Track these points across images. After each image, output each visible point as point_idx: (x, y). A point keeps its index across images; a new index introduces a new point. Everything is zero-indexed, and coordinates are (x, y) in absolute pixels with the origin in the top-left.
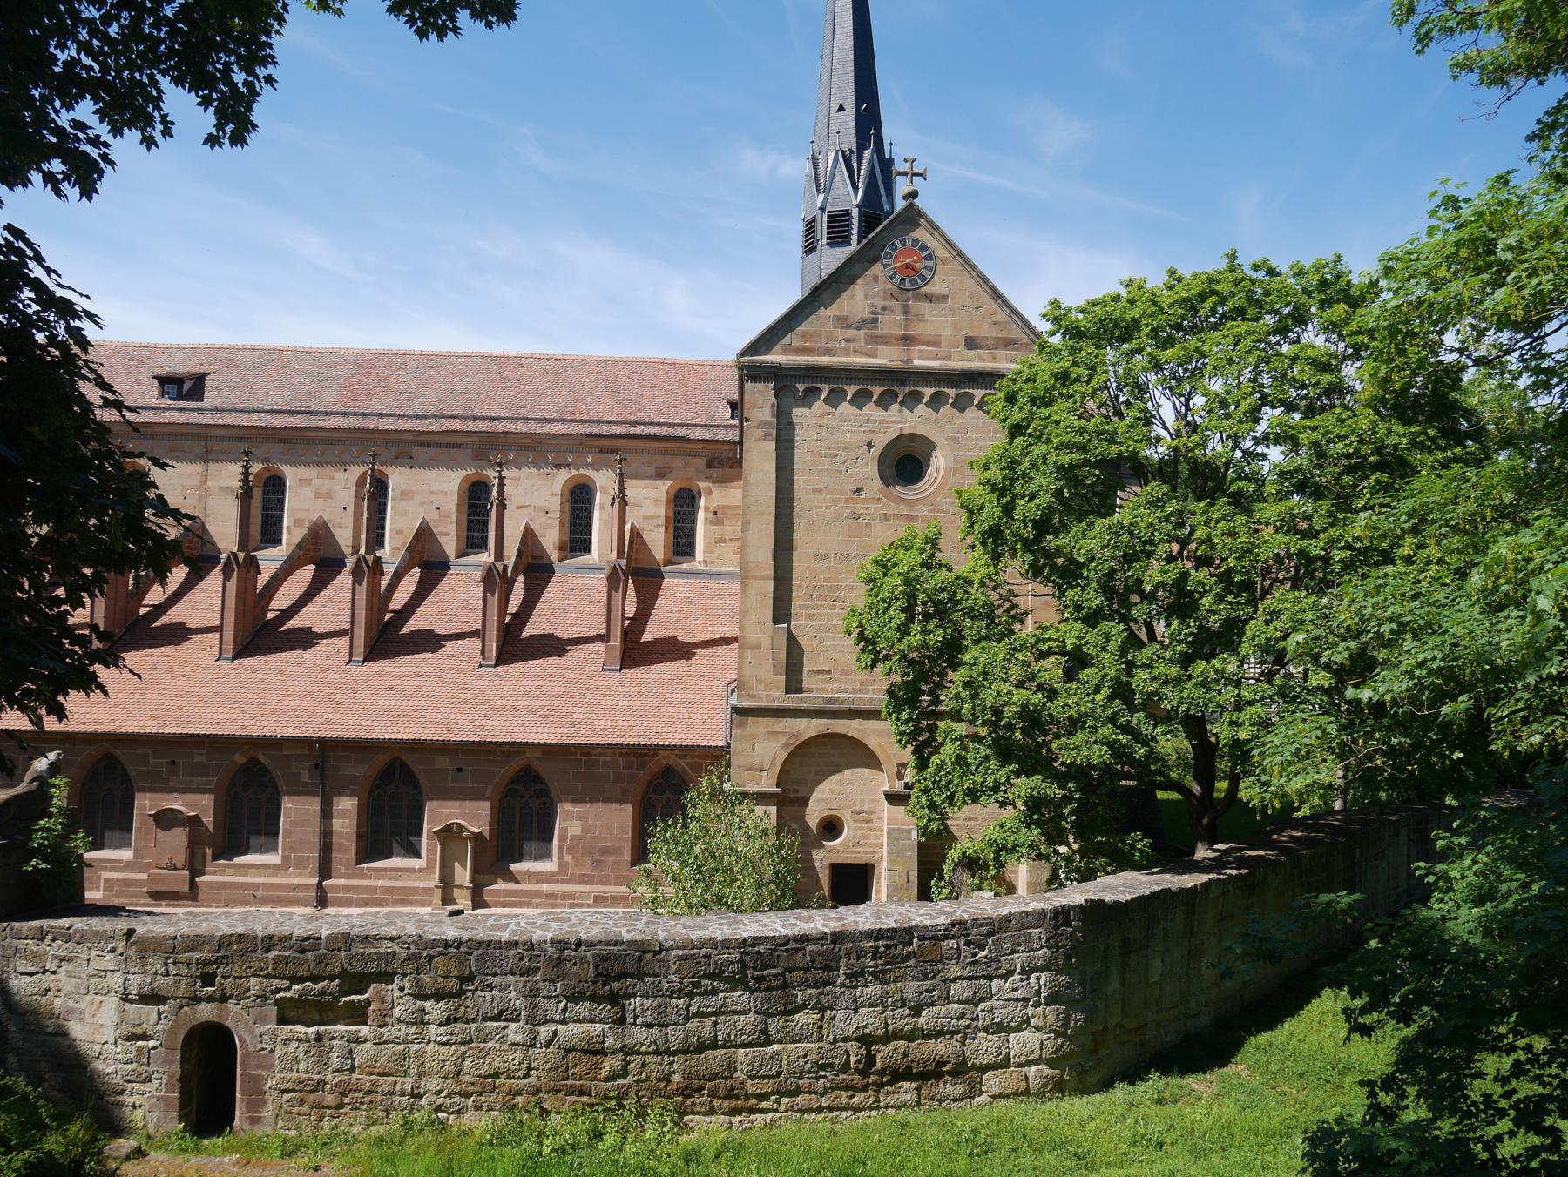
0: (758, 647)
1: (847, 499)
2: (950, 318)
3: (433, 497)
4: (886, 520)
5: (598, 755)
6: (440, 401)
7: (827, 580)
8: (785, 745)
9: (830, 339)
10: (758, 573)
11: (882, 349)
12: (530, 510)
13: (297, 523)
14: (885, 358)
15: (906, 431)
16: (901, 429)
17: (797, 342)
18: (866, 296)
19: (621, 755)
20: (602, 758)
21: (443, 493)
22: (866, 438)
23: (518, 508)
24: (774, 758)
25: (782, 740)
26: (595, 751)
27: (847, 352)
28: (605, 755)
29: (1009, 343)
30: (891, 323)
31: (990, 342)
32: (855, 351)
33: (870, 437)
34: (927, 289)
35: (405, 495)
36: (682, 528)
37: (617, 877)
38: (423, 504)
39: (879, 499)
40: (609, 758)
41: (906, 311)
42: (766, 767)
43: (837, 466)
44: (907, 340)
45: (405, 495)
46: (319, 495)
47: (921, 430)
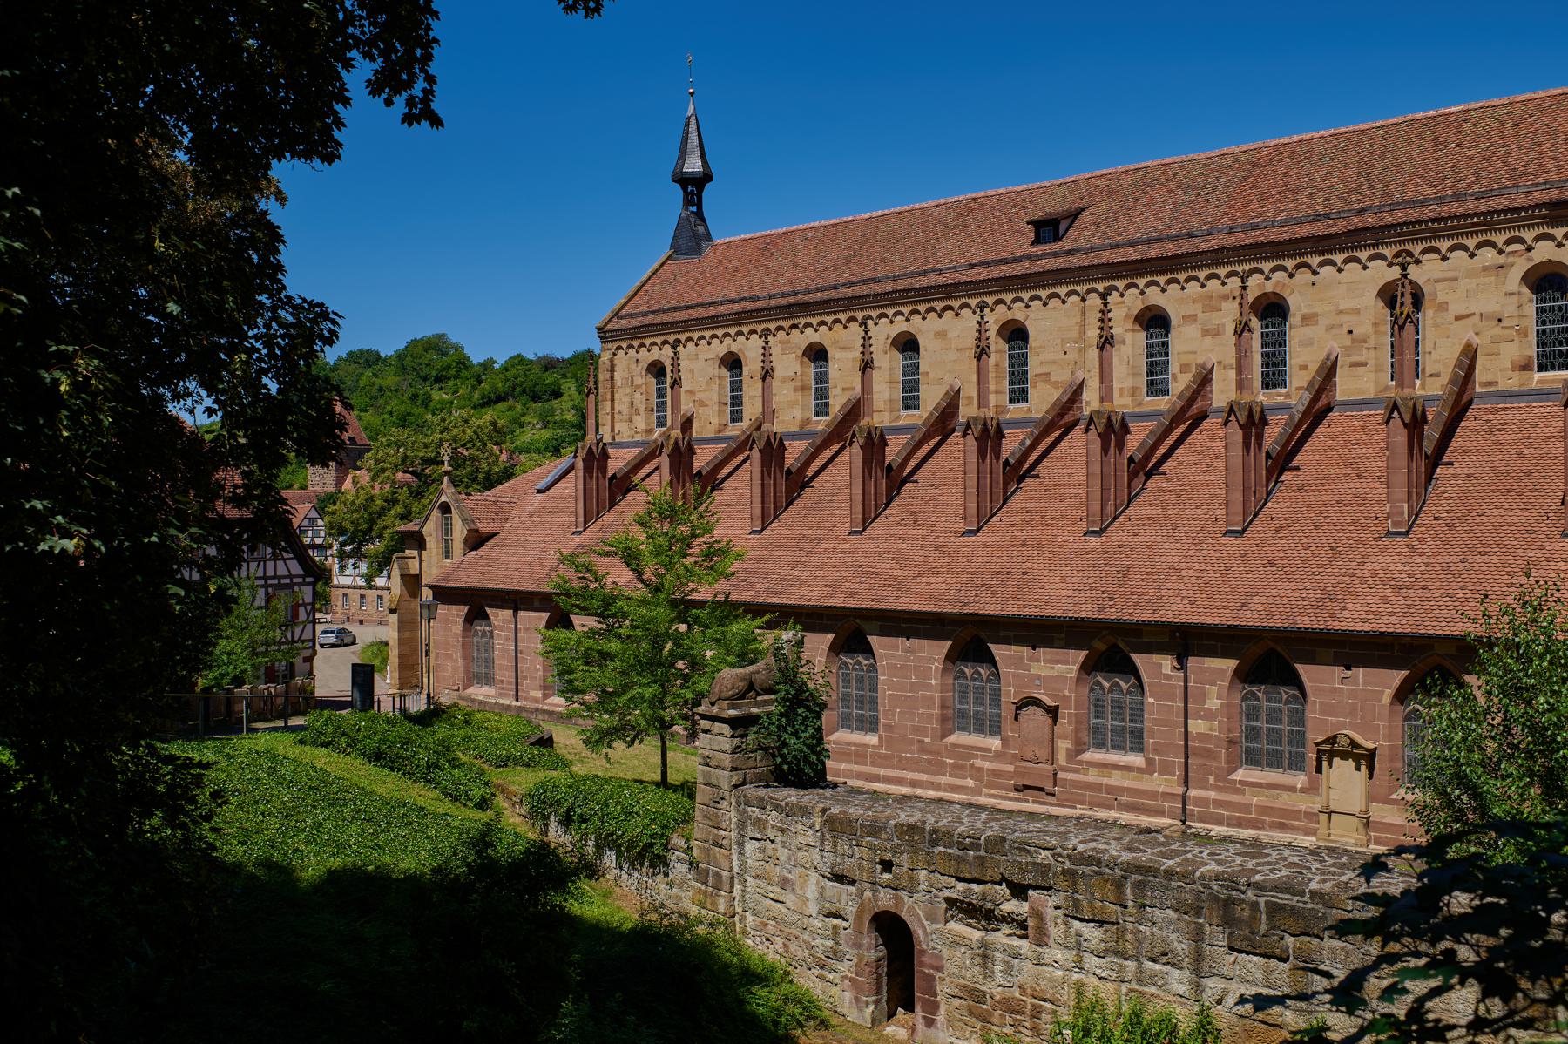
3: (1344, 318)
6: (1350, 192)
12: (1476, 319)
13: (1184, 368)
21: (1357, 311)
23: (1457, 318)
35: (1308, 319)
38: (1330, 328)
45: (1308, 319)
46: (1206, 333)
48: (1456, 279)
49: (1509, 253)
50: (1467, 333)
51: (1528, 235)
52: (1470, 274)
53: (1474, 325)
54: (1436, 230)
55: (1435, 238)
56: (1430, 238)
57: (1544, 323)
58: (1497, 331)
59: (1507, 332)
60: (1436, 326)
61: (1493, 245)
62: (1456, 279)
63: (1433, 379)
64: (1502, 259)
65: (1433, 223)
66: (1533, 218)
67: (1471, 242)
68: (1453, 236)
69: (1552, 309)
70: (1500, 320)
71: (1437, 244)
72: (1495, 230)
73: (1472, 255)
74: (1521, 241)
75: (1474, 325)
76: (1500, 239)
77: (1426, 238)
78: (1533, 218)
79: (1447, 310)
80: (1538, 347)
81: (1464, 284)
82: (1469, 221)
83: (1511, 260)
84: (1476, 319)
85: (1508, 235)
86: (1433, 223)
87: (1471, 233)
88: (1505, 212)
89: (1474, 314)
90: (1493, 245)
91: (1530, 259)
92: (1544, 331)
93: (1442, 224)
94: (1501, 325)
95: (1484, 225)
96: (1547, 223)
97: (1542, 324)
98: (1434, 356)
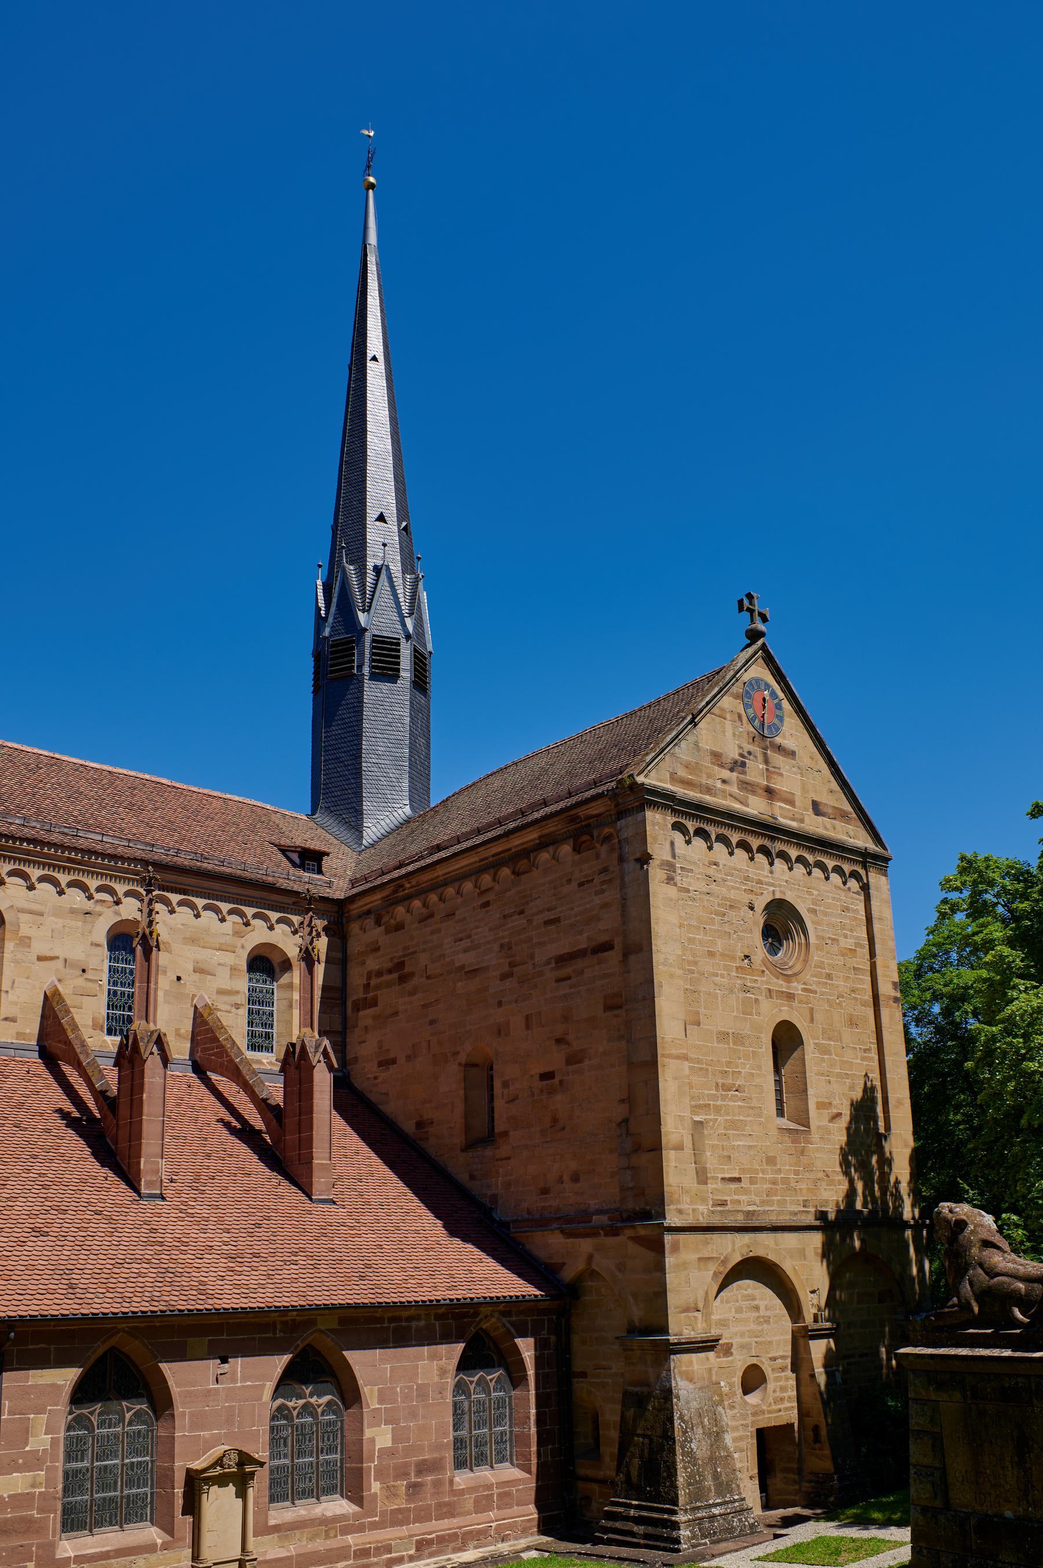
0: (679, 1147)
1: (737, 968)
2: (799, 777)
4: (771, 997)
5: (410, 1319)
7: (729, 1064)
8: (715, 1274)
9: (709, 776)
10: (674, 1052)
11: (753, 799)
12: (59, 964)
14: (755, 807)
15: (778, 896)
16: (774, 892)
17: (682, 773)
18: (734, 734)
19: (438, 1317)
20: (414, 1324)
22: (746, 898)
23: (40, 959)
24: (707, 1293)
25: (713, 1267)
26: (405, 1314)
27: (725, 794)
28: (418, 1318)
29: (843, 816)
30: (755, 772)
31: (830, 811)
32: (731, 795)
33: (752, 897)
34: (778, 740)
36: (258, 1012)
37: (440, 1506)
39: (763, 971)
40: (422, 1323)
41: (766, 761)
42: (701, 1306)
43: (727, 928)
44: (770, 793)
47: (790, 897)
48: (41, 914)
49: (98, 901)
50: (46, 978)
51: (121, 888)
52: (57, 912)
53: (57, 970)
54: (28, 852)
55: (25, 861)
56: (20, 860)
57: (115, 984)
58: (80, 982)
59: (90, 985)
60: (16, 962)
61: (84, 888)
62: (41, 914)
63: (8, 1023)
64: (89, 905)
65: (29, 844)
66: (127, 871)
67: (63, 878)
68: (44, 865)
69: (124, 970)
70: (84, 971)
71: (28, 870)
72: (89, 872)
73: (61, 893)
74: (112, 892)
75: (57, 970)
76: (93, 883)
77: (15, 859)
78: (127, 871)
79: (29, 947)
80: (108, 1009)
81: (51, 922)
82: (66, 854)
83: (99, 908)
84: (59, 964)
85: (72, 877)
86: (29, 844)
87: (64, 868)
88: (104, 855)
89: (58, 958)
90: (84, 888)
91: (117, 913)
92: (115, 992)
93: (38, 849)
94: (86, 976)
95: (79, 864)
96: (137, 880)
97: (114, 985)
98: (11, 997)
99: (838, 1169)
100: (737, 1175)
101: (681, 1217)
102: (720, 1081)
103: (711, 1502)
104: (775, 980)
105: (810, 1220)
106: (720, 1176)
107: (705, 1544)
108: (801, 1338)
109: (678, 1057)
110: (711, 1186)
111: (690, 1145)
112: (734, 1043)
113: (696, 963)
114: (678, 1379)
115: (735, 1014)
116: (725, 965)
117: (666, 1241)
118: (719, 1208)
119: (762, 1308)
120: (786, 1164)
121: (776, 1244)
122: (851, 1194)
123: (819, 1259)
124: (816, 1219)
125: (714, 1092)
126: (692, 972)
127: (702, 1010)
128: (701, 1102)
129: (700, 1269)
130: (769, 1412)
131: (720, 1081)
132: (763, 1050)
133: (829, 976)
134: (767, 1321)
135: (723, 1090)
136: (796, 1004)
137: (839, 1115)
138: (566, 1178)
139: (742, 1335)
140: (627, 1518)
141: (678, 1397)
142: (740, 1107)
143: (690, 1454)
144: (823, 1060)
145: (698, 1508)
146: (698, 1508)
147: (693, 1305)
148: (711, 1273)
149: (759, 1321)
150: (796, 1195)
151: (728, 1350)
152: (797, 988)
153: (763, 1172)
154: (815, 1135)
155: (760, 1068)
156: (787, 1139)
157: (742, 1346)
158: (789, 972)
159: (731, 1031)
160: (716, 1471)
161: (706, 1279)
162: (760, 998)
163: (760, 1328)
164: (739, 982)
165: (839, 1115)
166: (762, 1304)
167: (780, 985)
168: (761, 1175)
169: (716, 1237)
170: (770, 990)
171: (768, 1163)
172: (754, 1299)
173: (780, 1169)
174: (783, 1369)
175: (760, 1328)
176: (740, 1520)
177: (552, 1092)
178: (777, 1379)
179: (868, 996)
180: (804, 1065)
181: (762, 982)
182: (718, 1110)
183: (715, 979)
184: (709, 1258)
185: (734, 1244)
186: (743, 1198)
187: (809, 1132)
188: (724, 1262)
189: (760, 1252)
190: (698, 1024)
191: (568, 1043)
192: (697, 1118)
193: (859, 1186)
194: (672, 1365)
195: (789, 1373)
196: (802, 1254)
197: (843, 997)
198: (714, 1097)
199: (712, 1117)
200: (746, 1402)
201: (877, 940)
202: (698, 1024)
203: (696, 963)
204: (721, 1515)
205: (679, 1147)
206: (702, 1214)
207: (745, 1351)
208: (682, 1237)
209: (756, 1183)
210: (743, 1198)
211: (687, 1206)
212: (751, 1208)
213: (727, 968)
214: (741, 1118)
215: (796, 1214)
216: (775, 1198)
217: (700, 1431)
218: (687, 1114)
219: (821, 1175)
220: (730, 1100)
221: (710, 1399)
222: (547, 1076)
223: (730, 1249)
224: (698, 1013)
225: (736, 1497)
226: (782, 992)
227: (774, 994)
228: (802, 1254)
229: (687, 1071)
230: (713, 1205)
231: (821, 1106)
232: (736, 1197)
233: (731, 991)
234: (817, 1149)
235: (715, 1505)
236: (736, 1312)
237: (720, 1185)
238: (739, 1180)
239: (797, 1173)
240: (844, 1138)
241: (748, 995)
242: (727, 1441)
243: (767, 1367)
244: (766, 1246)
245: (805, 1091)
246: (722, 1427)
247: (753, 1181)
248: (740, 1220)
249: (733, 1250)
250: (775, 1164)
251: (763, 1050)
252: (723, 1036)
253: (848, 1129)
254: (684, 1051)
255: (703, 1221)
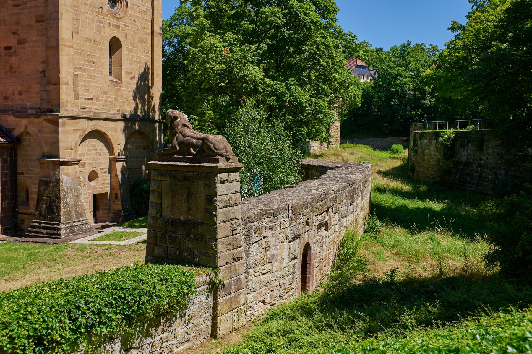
0: (67, 84)
1: (96, 12)
4: (110, 26)
7: (90, 52)
8: (80, 136)
10: (67, 44)
24: (76, 143)
25: (79, 133)
39: (107, 15)
42: (73, 148)
99: (132, 98)
100: (91, 98)
101: (67, 112)
102: (86, 59)
103: (74, 221)
104: (112, 19)
105: (119, 117)
106: (84, 97)
107: (71, 236)
108: (113, 161)
109: (68, 46)
110: (80, 101)
111: (72, 84)
112: (93, 43)
113: (78, 7)
114: (63, 175)
115: (94, 31)
116: (91, 10)
117: (60, 122)
118: (83, 110)
119: (98, 150)
120: (111, 95)
121: (105, 125)
122: (136, 108)
123: (122, 132)
124: (122, 117)
125: (83, 63)
126: (76, 10)
127: (80, 28)
128: (78, 66)
129: (74, 134)
130: (99, 188)
131: (86, 59)
132: (105, 48)
133: (135, 21)
134: (100, 154)
135: (87, 62)
136: (120, 30)
137: (134, 77)
138: (16, 93)
139: (90, 159)
140: (39, 227)
141: (62, 182)
142: (94, 70)
143: (67, 203)
144: (130, 55)
145: (69, 223)
146: (69, 223)
147: (70, 147)
148: (78, 135)
149: (96, 154)
150: (115, 107)
151: (84, 165)
152: (121, 23)
153: (102, 97)
154: (124, 84)
155: (103, 55)
156: (112, 85)
157: (90, 164)
158: (118, 17)
159: (92, 38)
160: (77, 209)
161: (76, 137)
162: (105, 26)
163: (97, 157)
164: (97, 18)
165: (134, 77)
166: (98, 148)
167: (114, 21)
168: (101, 98)
169: (81, 121)
170: (110, 23)
171: (104, 94)
172: (95, 146)
173: (109, 97)
174: (105, 173)
175: (97, 157)
176: (85, 227)
177: (10, 55)
178: (102, 176)
179: (150, 31)
180: (122, 56)
181: (107, 19)
182: (85, 70)
183: (86, 15)
184: (78, 129)
185: (88, 124)
186: (93, 107)
187: (122, 83)
188: (84, 131)
189: (99, 128)
190: (78, 33)
191: (18, 35)
192: (75, 73)
193: (140, 106)
194: (60, 170)
195: (107, 174)
196: (115, 130)
197: (139, 30)
198: (83, 65)
199: (82, 73)
200: (90, 185)
201: (155, 9)
202: (78, 33)
203: (78, 7)
204: (78, 225)
205: (67, 84)
206: (76, 112)
207: (90, 165)
208: (67, 120)
209: (99, 101)
210: (93, 107)
211: (69, 108)
212: (96, 111)
213: (91, 11)
214: (94, 74)
215: (114, 114)
216: (106, 108)
217: (71, 195)
218: (71, 71)
219: (125, 100)
220: (90, 67)
221: (76, 183)
222: (8, 48)
223: (86, 126)
224: (78, 29)
225: (84, 219)
226: (115, 25)
227: (111, 25)
228: (115, 130)
229: (72, 53)
230: (80, 109)
231: (127, 73)
232: (90, 106)
233: (93, 21)
234: (124, 90)
235: (76, 222)
236: (88, 151)
237: (84, 101)
238: (92, 99)
239: (116, 98)
240: (135, 87)
241: (100, 24)
242: (81, 198)
243: (99, 172)
244: (101, 126)
245: (121, 66)
246: (80, 193)
247: (97, 100)
248: (91, 115)
249: (88, 127)
250: (107, 94)
251: (105, 48)
252: (88, 40)
253: (137, 83)
254: (71, 44)
255: (76, 115)
